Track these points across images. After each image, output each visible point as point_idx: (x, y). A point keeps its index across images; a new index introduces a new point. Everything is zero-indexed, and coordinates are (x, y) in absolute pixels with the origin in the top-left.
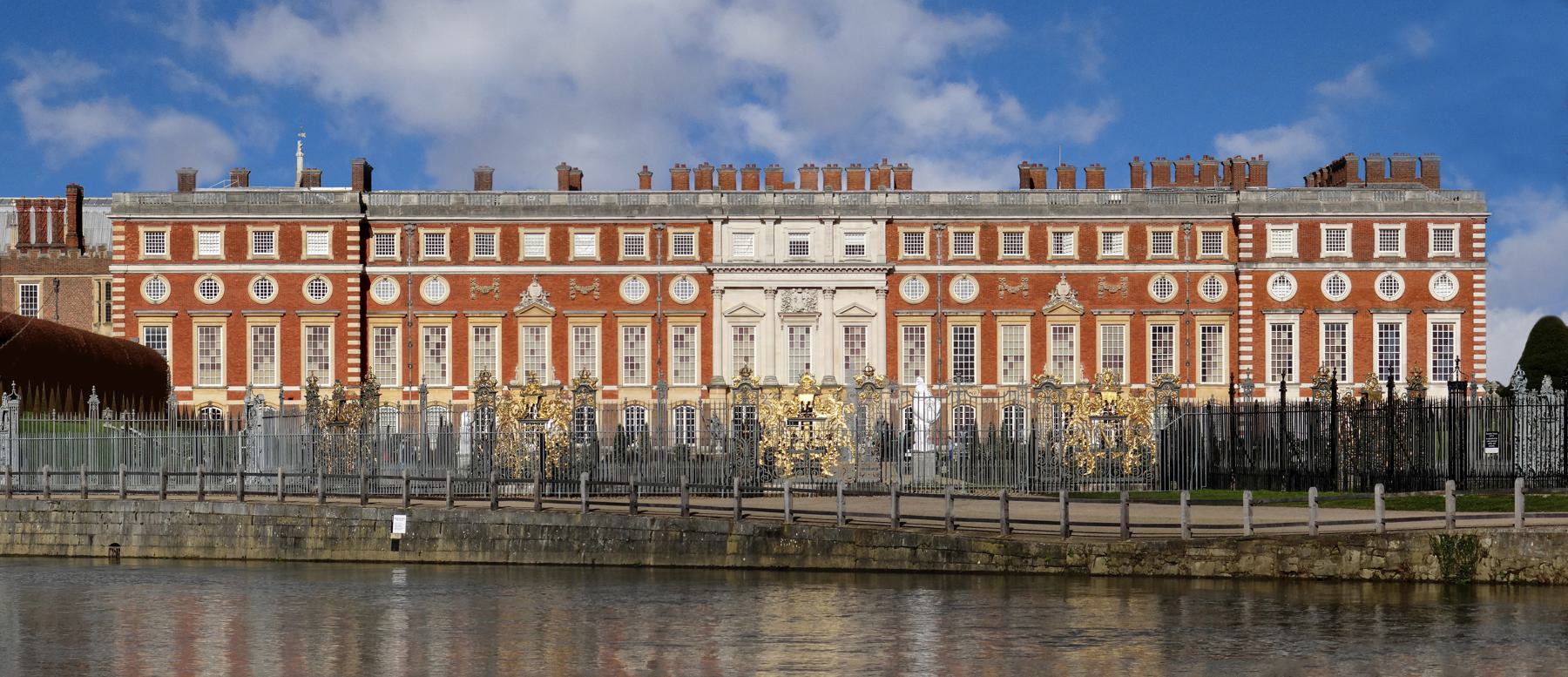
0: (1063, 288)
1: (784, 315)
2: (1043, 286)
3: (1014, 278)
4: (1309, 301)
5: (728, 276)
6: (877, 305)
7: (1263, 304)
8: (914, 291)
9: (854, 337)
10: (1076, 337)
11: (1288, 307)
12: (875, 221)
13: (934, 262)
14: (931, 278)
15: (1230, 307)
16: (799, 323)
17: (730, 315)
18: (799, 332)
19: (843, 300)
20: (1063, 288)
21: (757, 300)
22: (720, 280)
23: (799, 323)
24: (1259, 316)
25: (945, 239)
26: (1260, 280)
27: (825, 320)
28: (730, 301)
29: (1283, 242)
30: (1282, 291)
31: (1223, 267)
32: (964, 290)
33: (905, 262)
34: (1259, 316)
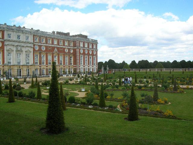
0: (56, 49)
1: (17, 51)
2: (54, 48)
3: (50, 47)
4: (84, 54)
5: (8, 42)
6: (32, 50)
7: (80, 53)
8: (37, 48)
9: (27, 56)
10: (57, 57)
11: (82, 54)
12: (31, 34)
13: (39, 43)
14: (39, 46)
15: (75, 54)
16: (19, 52)
17: (8, 50)
18: (19, 54)
19: (27, 49)
20: (56, 49)
21: (12, 48)
22: (6, 43)
23: (19, 52)
24: (79, 55)
25: (41, 39)
26: (80, 49)
27: (24, 52)
28: (8, 47)
29: (82, 45)
30: (82, 51)
31: (72, 48)
32: (44, 49)
33: (36, 43)
34: (79, 55)
